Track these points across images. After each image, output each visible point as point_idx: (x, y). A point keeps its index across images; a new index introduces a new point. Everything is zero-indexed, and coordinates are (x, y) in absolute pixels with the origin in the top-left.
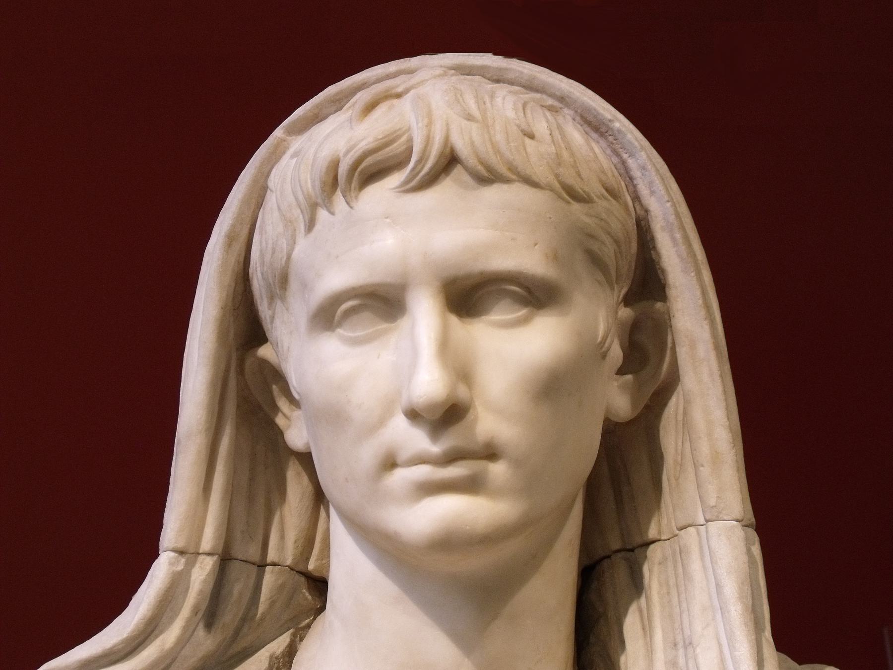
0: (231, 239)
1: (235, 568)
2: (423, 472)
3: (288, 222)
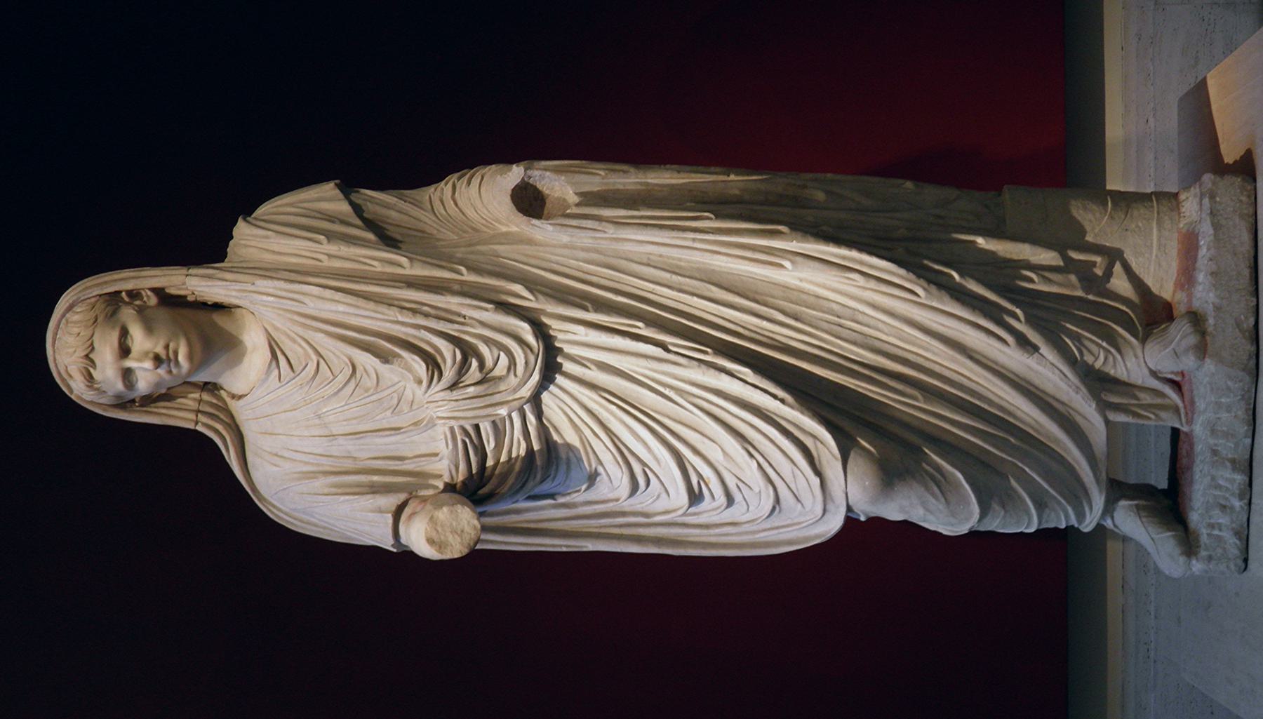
0: (105, 410)
1: (201, 408)
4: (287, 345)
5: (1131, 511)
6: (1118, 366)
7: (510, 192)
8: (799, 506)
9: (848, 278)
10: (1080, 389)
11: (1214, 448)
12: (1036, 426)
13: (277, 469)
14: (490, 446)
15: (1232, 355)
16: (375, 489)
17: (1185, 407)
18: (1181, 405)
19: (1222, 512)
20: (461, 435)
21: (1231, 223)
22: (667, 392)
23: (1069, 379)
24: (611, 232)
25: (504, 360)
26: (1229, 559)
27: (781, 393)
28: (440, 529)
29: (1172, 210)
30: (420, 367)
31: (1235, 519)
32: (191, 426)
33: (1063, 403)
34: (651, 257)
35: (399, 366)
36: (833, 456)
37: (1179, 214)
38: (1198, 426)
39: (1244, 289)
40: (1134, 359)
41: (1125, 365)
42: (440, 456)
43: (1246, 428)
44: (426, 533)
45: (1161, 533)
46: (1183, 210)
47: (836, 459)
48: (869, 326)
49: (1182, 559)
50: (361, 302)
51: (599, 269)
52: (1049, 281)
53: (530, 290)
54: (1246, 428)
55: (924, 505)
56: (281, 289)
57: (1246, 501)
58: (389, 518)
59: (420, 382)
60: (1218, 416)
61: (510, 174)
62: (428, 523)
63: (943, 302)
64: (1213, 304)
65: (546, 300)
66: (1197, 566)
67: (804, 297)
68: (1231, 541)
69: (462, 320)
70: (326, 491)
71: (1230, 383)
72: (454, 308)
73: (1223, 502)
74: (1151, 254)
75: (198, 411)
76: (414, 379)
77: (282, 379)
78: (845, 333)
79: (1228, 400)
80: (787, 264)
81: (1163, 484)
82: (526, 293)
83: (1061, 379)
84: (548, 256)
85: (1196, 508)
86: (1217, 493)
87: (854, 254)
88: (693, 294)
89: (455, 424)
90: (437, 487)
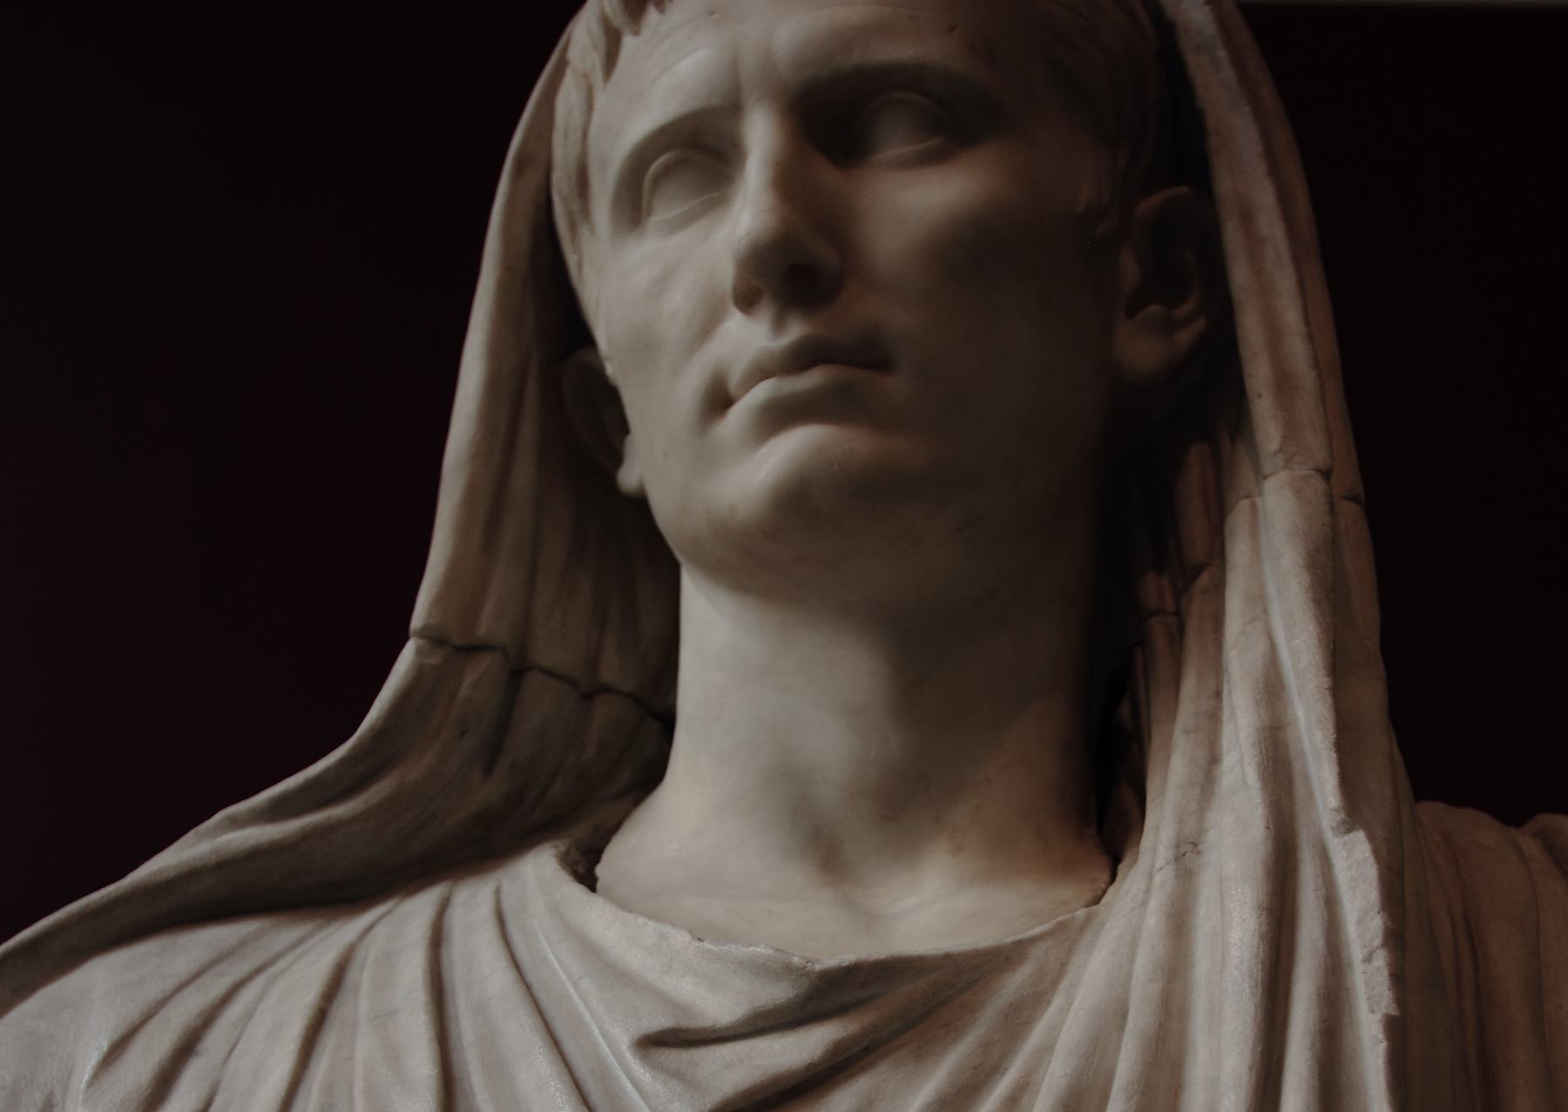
2: (762, 391)
32: (418, 619)
75: (517, 673)
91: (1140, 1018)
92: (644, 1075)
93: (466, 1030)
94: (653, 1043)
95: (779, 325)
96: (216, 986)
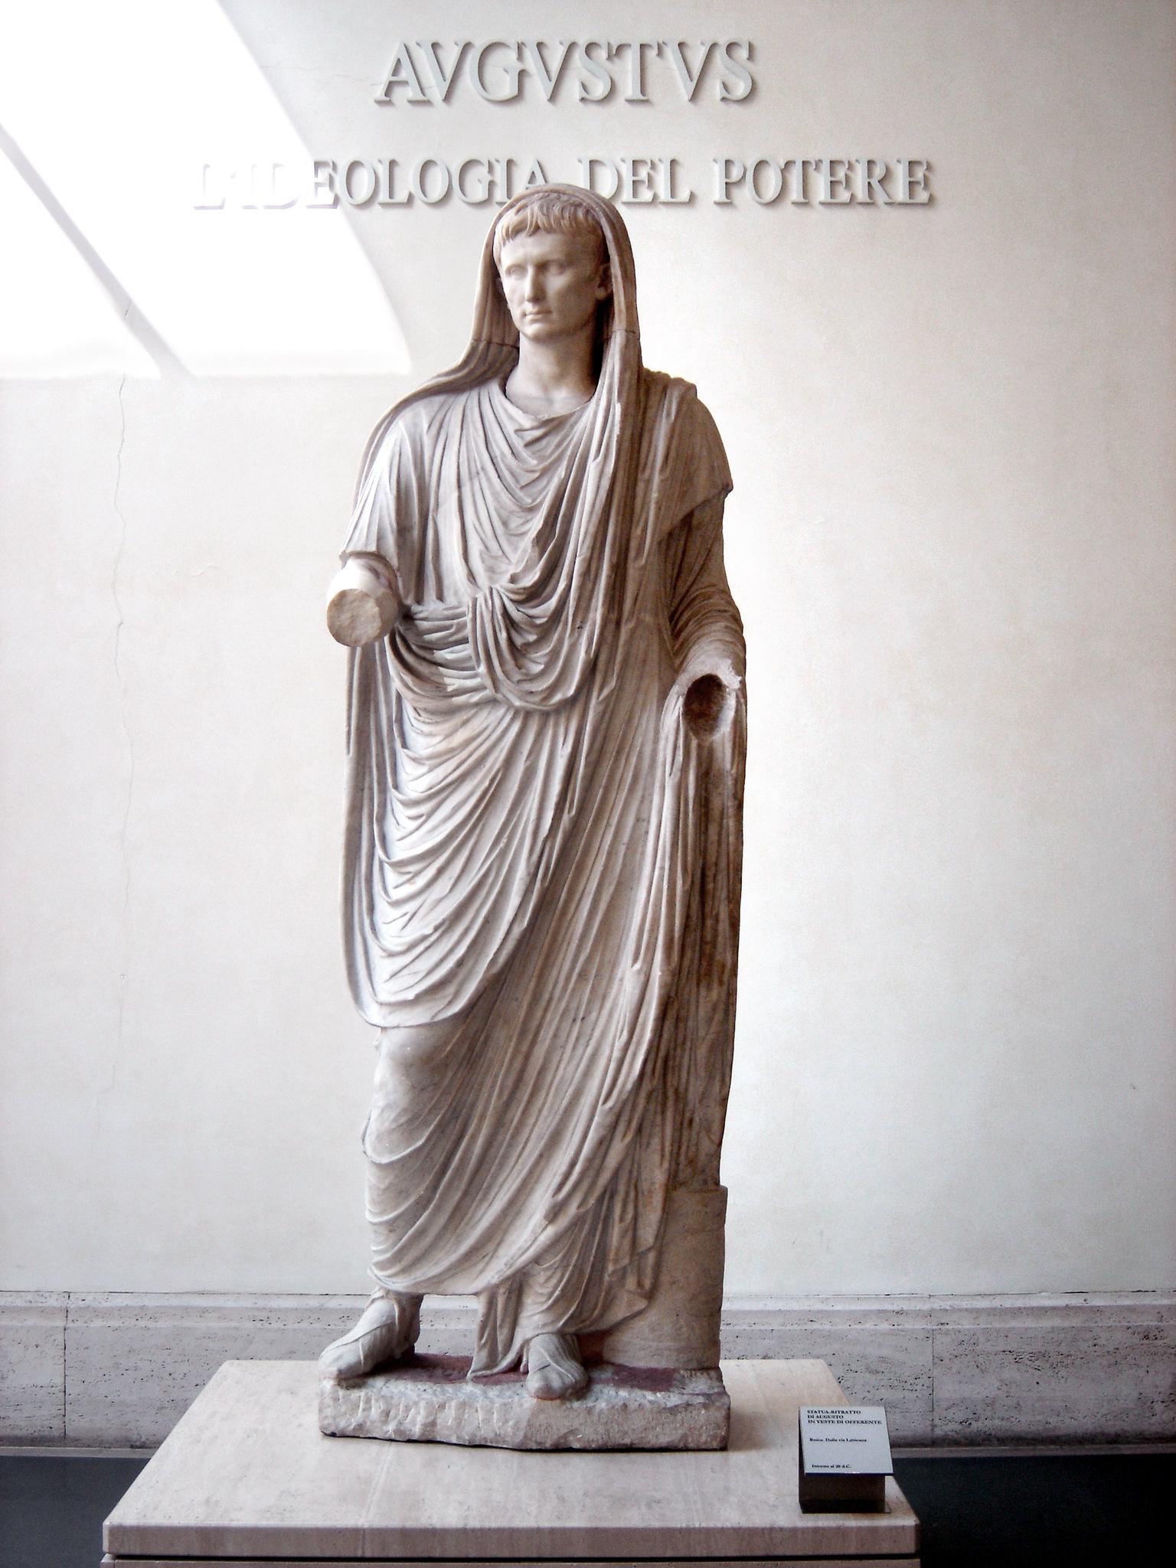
3: (499, 243)
4: (554, 440)
5: (388, 1317)
6: (536, 1306)
7: (714, 673)
8: (388, 977)
9: (622, 1031)
10: (510, 1268)
11: (447, 1405)
12: (472, 1223)
13: (425, 426)
14: (446, 655)
15: (540, 1426)
16: (402, 530)
17: (492, 1375)
18: (496, 1370)
19: (383, 1411)
20: (458, 624)
21: (678, 1425)
22: (504, 840)
23: (521, 1256)
24: (670, 782)
25: (537, 668)
26: (335, 1418)
27: (502, 959)
28: (356, 603)
29: (699, 1362)
30: (530, 579)
31: (375, 1424)
33: (495, 1251)
34: (645, 824)
35: (530, 559)
36: (436, 1014)
37: (694, 1370)
38: (472, 1389)
39: (609, 1438)
40: (541, 1323)
41: (535, 1315)
42: (438, 602)
43: (467, 1438)
44: (351, 590)
45: (363, 1345)
46: (699, 1374)
47: (433, 1017)
48: (574, 1048)
49: (334, 1370)
50: (595, 520)
51: (632, 768)
52: (622, 1237)
53: (608, 697)
54: (467, 1438)
55: (388, 1106)
56: (611, 431)
57: (393, 1437)
58: (373, 548)
59: (513, 579)
60: (479, 1409)
61: (733, 673)
62: (362, 591)
63: (596, 1129)
64: (594, 1406)
65: (599, 713)
66: (329, 1385)
67: (604, 983)
68: (353, 1420)
69: (577, 626)
70: (403, 480)
71: (511, 1423)
72: (591, 615)
73: (392, 1414)
74: (653, 1341)
75: (489, 343)
76: (517, 573)
77: (520, 433)
78: (566, 1025)
79: (495, 1421)
80: (638, 966)
81: (420, 1348)
82: (606, 692)
83: (519, 1249)
84: (646, 715)
85: (388, 1385)
86: (402, 1408)
87: (648, 1035)
88: (606, 867)
89: (468, 618)
90: (407, 596)
91: (587, 430)
92: (516, 436)
93: (487, 425)
94: (517, 431)
95: (534, 306)
96: (443, 413)
